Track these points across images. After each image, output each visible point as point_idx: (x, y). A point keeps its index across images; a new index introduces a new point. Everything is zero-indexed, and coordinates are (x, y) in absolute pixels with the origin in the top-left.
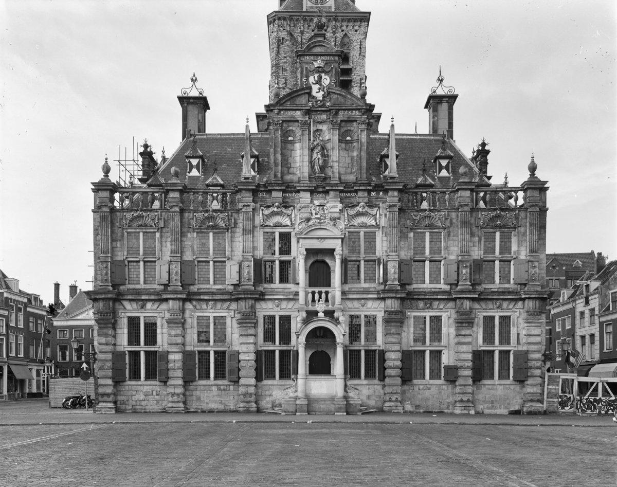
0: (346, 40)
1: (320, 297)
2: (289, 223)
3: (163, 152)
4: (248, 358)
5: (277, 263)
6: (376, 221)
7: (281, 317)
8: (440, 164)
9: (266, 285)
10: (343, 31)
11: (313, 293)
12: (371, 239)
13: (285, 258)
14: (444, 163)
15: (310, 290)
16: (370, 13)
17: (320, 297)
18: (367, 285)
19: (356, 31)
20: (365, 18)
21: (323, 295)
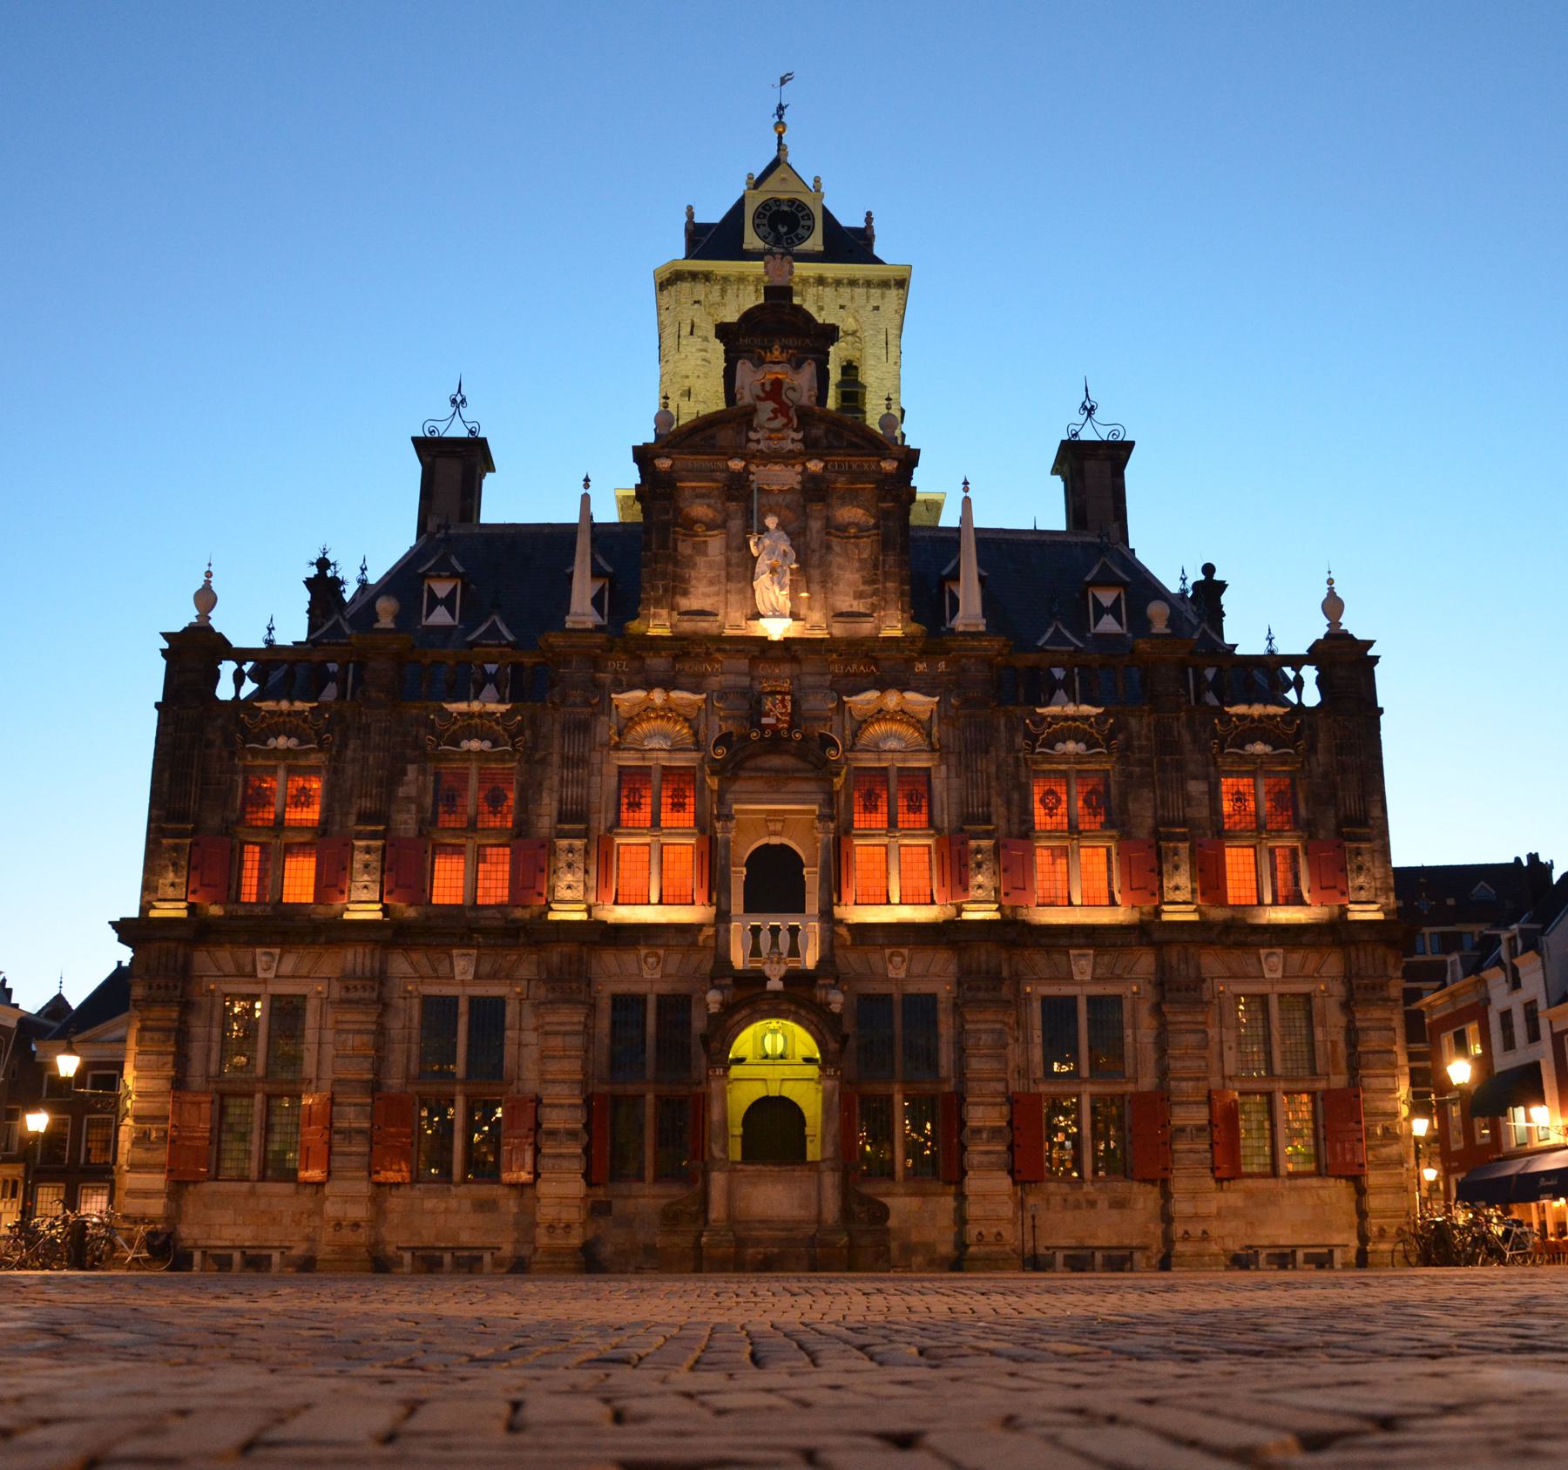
1: (775, 944)
4: (564, 1115)
6: (929, 735)
7: (660, 997)
8: (1095, 599)
11: (756, 931)
14: (1107, 597)
17: (775, 944)
21: (784, 939)
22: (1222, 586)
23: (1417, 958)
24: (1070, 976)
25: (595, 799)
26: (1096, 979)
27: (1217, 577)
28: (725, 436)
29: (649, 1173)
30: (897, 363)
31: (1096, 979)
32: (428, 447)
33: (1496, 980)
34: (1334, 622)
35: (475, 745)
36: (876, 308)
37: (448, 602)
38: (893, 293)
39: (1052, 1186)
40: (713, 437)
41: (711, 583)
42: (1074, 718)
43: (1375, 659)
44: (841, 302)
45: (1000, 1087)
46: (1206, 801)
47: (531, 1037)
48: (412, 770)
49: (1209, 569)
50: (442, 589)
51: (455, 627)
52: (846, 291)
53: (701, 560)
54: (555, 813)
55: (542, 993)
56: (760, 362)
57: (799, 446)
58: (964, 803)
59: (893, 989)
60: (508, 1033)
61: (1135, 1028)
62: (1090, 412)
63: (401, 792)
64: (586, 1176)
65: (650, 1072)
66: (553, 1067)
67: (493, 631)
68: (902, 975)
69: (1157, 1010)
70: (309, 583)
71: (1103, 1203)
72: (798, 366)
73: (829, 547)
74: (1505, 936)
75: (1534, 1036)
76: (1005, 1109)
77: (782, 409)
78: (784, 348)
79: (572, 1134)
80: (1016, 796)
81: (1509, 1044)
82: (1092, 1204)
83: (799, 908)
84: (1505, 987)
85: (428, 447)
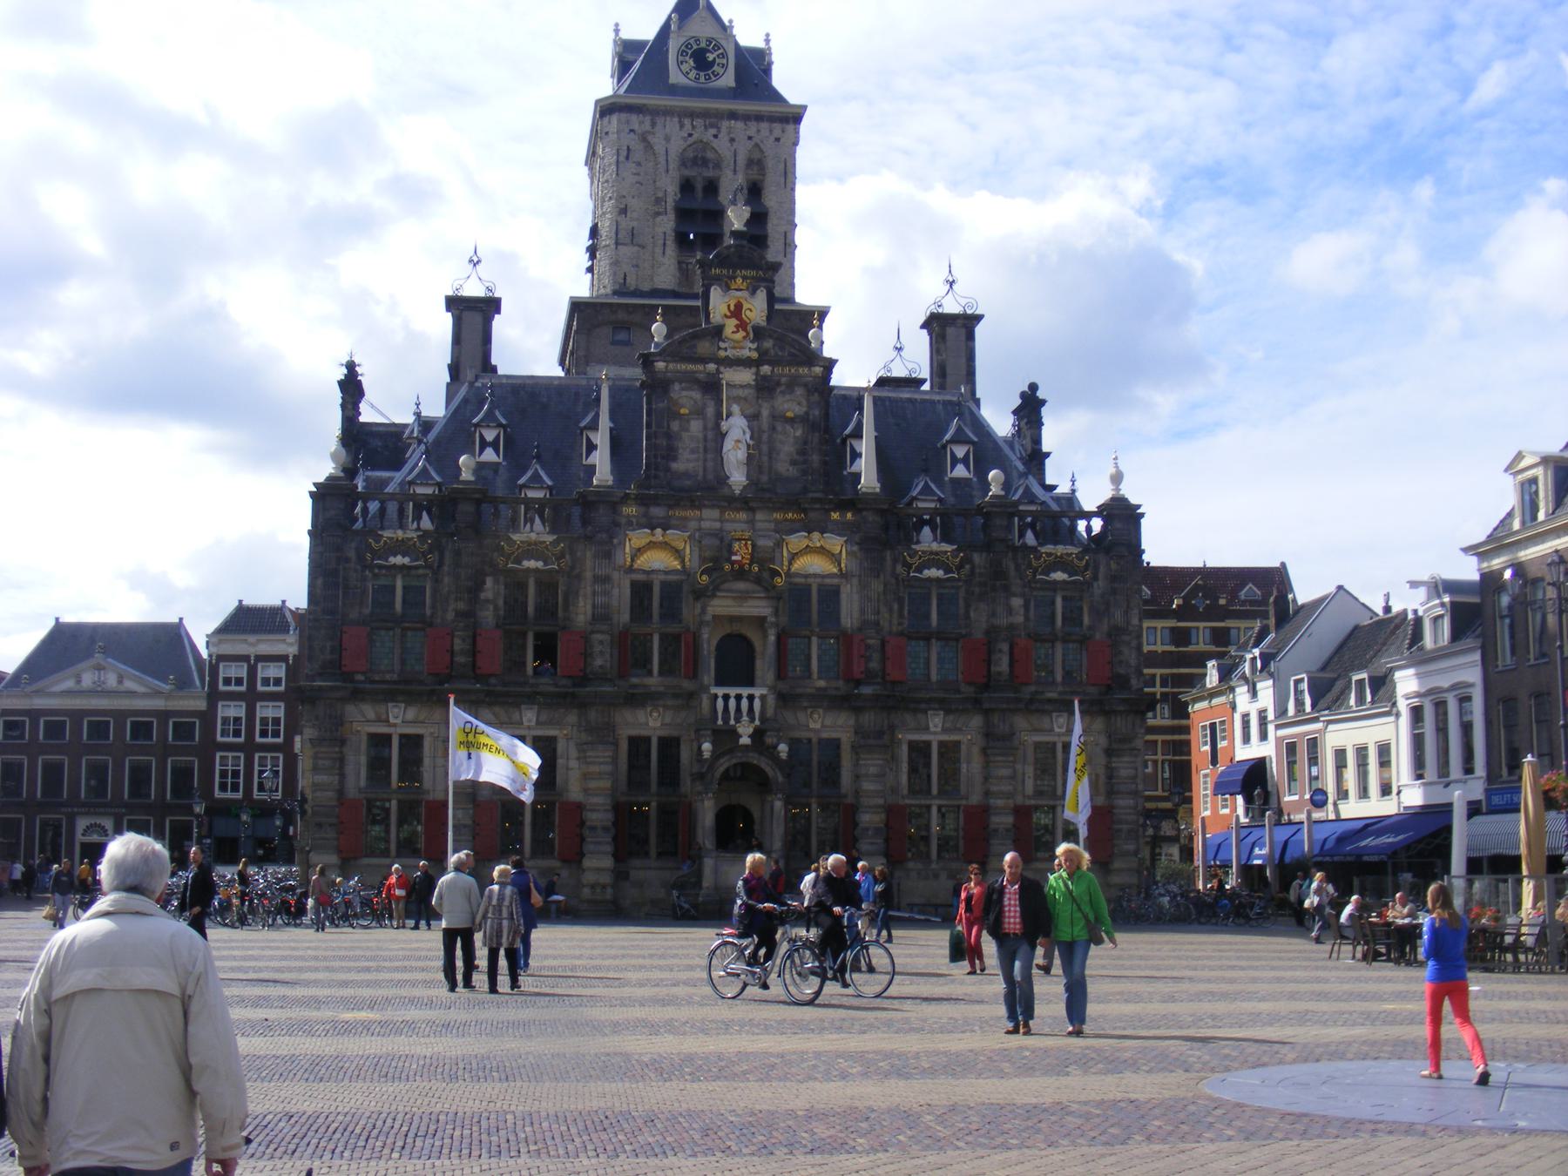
0: (756, 156)
2: (676, 565)
3: (418, 405)
4: (599, 815)
5: (656, 639)
7: (661, 739)
8: (953, 454)
9: (635, 680)
10: (750, 138)
11: (726, 697)
12: (830, 595)
13: (673, 629)
14: (960, 451)
15: (720, 691)
16: (804, 108)
18: (822, 683)
19: (778, 140)
20: (794, 117)
21: (745, 703)
22: (1043, 402)
23: (1191, 648)
24: (927, 728)
25: (615, 603)
26: (945, 730)
27: (1040, 394)
28: (704, 347)
29: (653, 852)
30: (793, 189)
31: (945, 730)
32: (455, 304)
33: (1242, 693)
34: (1118, 490)
35: (531, 564)
36: (778, 140)
37: (495, 445)
38: (790, 127)
39: (911, 865)
40: (695, 346)
41: (693, 451)
42: (937, 553)
43: (1142, 515)
44: (749, 133)
45: (881, 801)
46: (1022, 611)
47: (573, 764)
48: (489, 582)
49: (1033, 387)
50: (490, 435)
51: (498, 464)
52: (753, 128)
53: (685, 435)
54: (589, 612)
55: (584, 737)
56: (727, 288)
57: (755, 355)
58: (862, 612)
59: (811, 735)
60: (560, 762)
61: (969, 763)
62: (951, 284)
63: (483, 596)
64: (618, 857)
65: (654, 787)
66: (593, 784)
67: (536, 478)
68: (818, 726)
69: (984, 751)
70: (341, 383)
71: (943, 876)
72: (753, 293)
73: (774, 429)
74: (1249, 656)
75: (1264, 736)
76: (883, 816)
77: (742, 325)
78: (744, 278)
79: (605, 829)
80: (896, 607)
81: (1246, 739)
82: (936, 876)
83: (751, 684)
84: (1247, 697)
85: (455, 304)
